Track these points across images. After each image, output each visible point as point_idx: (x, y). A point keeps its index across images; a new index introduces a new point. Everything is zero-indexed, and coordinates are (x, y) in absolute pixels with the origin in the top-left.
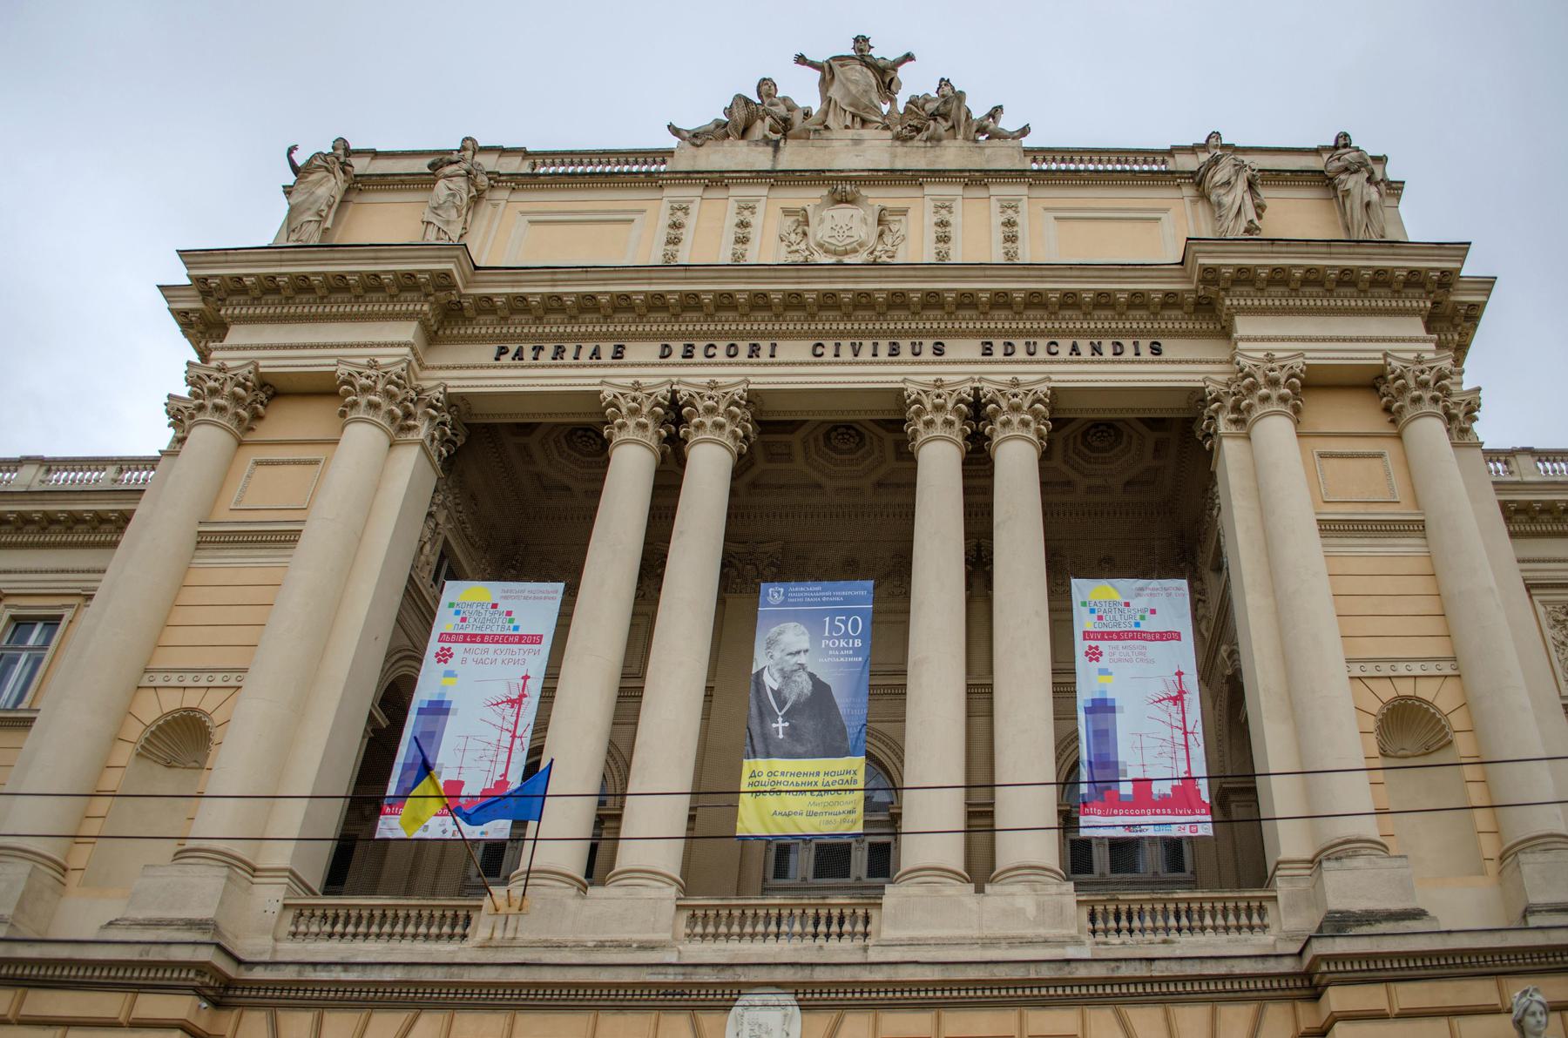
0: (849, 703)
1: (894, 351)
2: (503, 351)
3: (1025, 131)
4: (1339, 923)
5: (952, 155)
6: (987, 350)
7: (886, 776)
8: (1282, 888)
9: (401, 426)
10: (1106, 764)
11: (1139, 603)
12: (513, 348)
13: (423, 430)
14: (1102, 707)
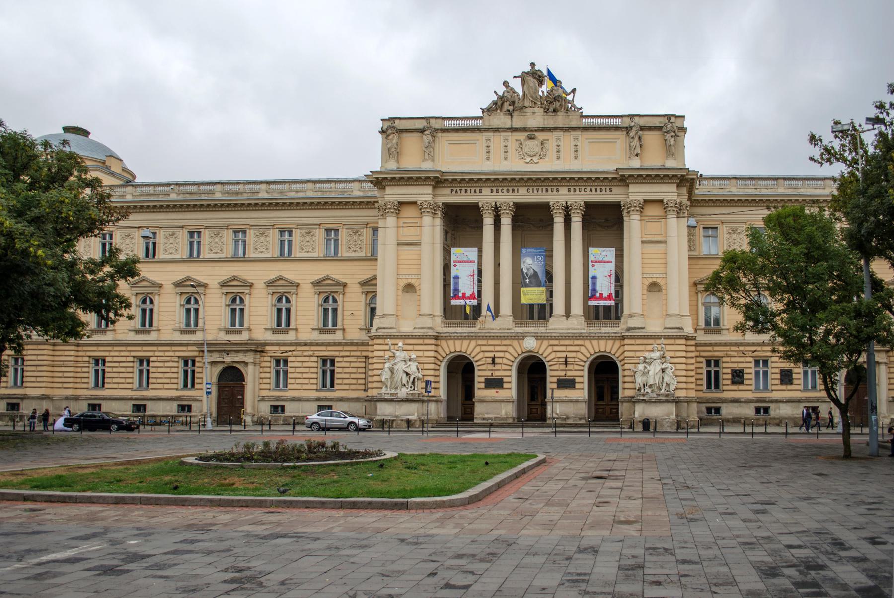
0: (542, 277)
1: (547, 191)
3: (581, 108)
4: (629, 329)
6: (569, 190)
7: (551, 294)
8: (622, 320)
10: (594, 290)
11: (604, 254)
14: (594, 278)
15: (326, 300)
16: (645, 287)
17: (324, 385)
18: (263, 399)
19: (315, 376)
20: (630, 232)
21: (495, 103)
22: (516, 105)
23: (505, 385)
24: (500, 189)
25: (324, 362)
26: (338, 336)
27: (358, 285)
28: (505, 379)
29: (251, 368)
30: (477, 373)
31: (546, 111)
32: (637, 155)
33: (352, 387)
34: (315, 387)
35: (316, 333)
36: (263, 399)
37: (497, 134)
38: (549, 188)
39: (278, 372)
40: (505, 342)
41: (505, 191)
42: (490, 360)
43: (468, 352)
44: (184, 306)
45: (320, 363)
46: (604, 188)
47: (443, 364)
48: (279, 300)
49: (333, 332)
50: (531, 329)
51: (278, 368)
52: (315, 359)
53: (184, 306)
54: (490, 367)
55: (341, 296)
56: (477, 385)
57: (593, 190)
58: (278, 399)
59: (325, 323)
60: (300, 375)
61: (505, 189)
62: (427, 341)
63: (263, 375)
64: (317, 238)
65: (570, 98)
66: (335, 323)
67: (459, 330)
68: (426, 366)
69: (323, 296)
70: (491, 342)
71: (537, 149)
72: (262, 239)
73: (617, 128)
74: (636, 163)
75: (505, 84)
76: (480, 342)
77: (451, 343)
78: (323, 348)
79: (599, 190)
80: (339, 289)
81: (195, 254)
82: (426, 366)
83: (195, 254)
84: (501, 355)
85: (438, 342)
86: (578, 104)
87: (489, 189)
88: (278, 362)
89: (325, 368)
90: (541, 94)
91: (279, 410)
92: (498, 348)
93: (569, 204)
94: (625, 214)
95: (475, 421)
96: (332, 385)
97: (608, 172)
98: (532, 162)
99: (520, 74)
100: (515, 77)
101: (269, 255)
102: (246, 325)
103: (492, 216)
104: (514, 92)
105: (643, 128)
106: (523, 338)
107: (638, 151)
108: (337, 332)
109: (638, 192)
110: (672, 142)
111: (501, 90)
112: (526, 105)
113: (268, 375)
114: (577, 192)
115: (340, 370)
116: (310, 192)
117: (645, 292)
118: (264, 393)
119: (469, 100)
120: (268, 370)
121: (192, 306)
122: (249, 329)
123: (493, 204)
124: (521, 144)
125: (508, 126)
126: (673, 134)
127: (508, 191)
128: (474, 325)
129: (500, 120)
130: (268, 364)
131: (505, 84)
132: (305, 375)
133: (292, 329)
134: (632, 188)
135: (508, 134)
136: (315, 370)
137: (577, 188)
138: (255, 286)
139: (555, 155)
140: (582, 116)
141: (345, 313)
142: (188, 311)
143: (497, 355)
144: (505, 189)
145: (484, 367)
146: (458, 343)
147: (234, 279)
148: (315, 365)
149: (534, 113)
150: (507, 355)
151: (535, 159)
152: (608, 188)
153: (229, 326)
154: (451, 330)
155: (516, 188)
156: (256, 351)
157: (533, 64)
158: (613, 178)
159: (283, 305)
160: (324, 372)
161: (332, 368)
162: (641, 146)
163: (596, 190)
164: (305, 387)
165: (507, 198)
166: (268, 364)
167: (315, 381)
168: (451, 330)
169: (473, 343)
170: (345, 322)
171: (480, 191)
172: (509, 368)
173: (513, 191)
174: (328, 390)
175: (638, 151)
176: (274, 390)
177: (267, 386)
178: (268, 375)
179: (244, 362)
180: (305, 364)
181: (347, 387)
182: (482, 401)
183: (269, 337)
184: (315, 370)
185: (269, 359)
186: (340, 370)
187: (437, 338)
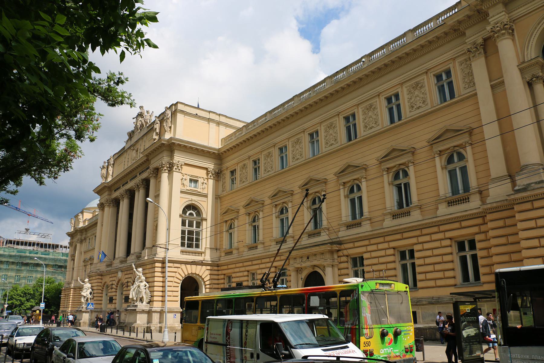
25: (461, 246)
34: (451, 282)
39: (404, 267)
52: (448, 242)
60: (430, 268)
64: (427, 88)
89: (463, 254)
108: (472, 198)
160: (463, 260)
161: (473, 252)
164: (439, 283)
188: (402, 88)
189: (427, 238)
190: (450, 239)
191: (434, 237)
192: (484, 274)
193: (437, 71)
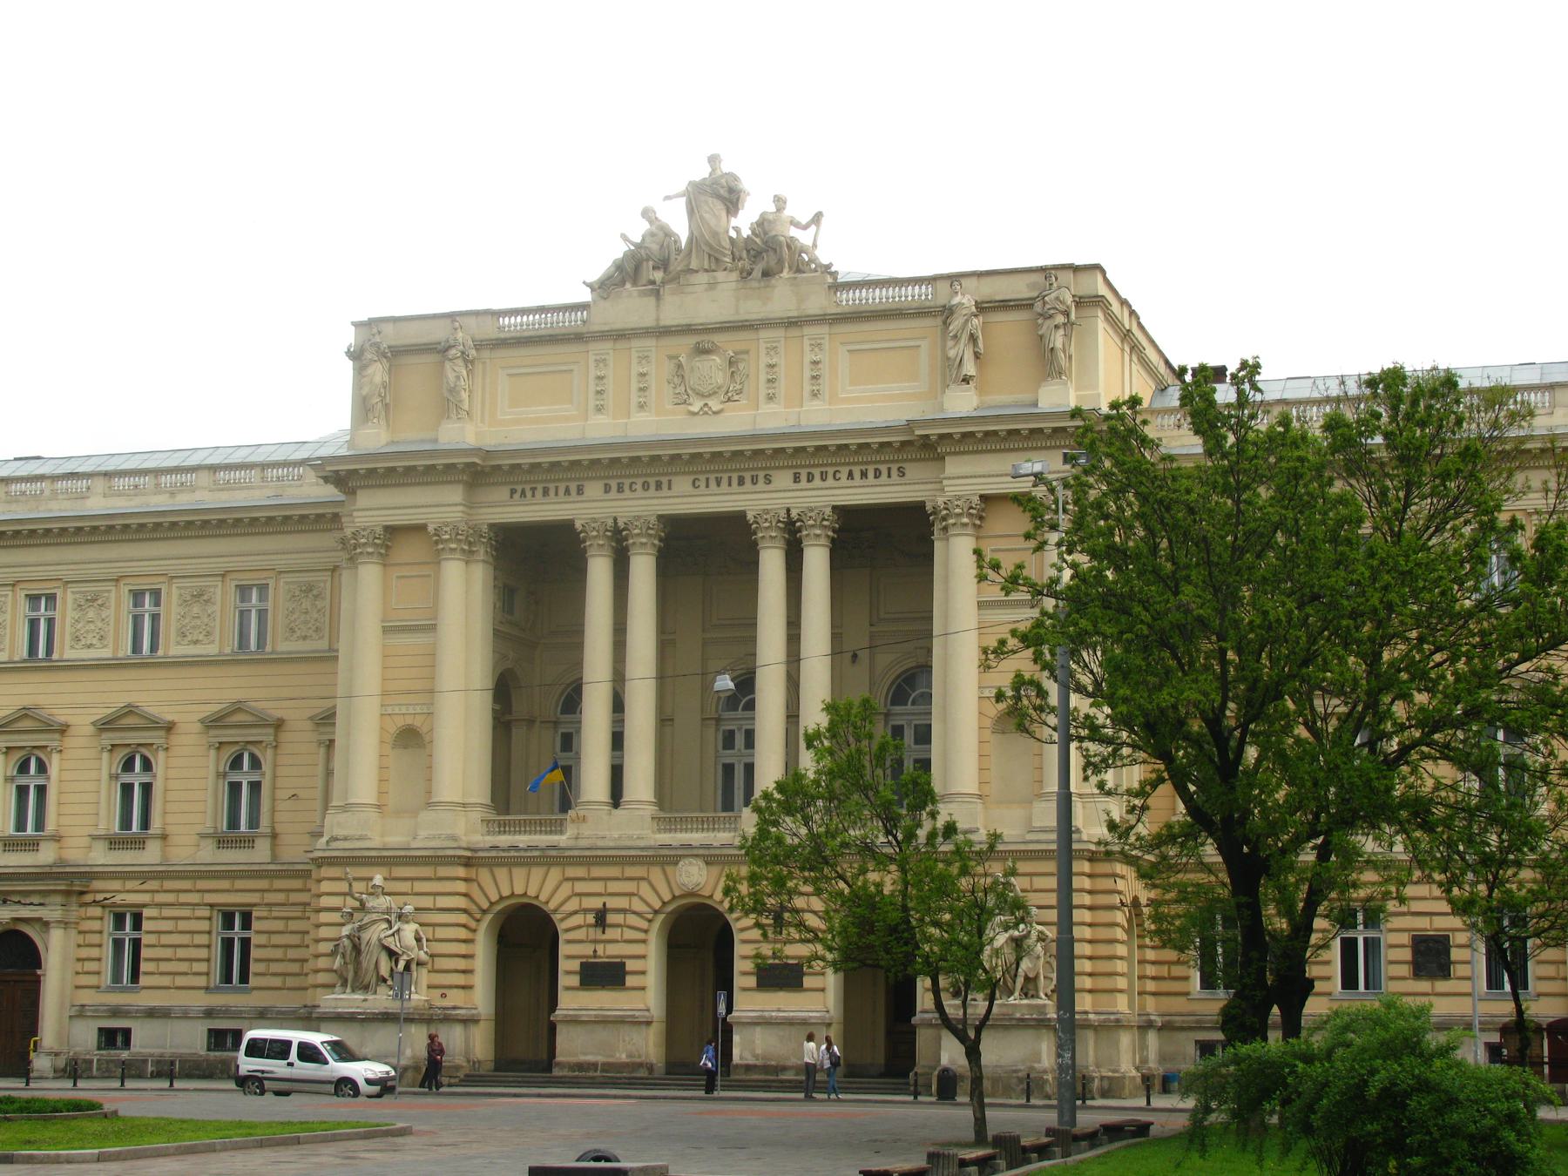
2: (513, 492)
5: (781, 299)
6: (797, 479)
9: (468, 556)
12: (519, 488)
13: (481, 555)
15: (236, 763)
16: (988, 723)
17: (227, 978)
18: (81, 1013)
19: (203, 953)
20: (946, 579)
21: (619, 266)
22: (671, 268)
23: (630, 981)
24: (627, 482)
26: (260, 853)
27: (309, 725)
28: (631, 965)
29: (56, 937)
30: (564, 949)
31: (746, 275)
32: (966, 380)
33: (290, 982)
34: (202, 981)
35: (209, 845)
36: (81, 1013)
37: (621, 345)
38: (747, 476)
39: (118, 944)
40: (631, 871)
41: (639, 487)
42: (591, 919)
43: (543, 898)
44: (117, 777)
45: (218, 921)
46: (883, 468)
47: (484, 925)
48: (128, 766)
49: (248, 842)
50: (696, 837)
51: (119, 935)
52: (206, 912)
53: (117, 777)
54: (595, 933)
55: (269, 752)
56: (563, 980)
57: (857, 475)
58: (116, 1012)
59: (234, 822)
60: (168, 953)
61: (640, 481)
62: (443, 871)
63: (85, 953)
64: (217, 607)
65: (804, 238)
66: (254, 822)
67: (523, 840)
68: (442, 933)
69: (228, 752)
70: (597, 871)
71: (720, 378)
72: (91, 614)
73: (921, 312)
74: (962, 403)
75: (647, 214)
76: (572, 872)
77: (501, 873)
78: (225, 884)
79: (871, 474)
80: (266, 735)
81: (41, 653)
82: (442, 933)
83: (41, 653)
84: (622, 903)
85: (472, 873)
86: (823, 257)
87: (600, 485)
88: (119, 920)
89: (229, 933)
90: (733, 234)
91: (119, 1039)
92: (614, 887)
93: (794, 514)
94: (937, 533)
95: (556, 1072)
96: (244, 978)
97: (888, 429)
98: (705, 411)
99: (682, 187)
100: (667, 198)
101: (106, 653)
102: (51, 826)
103: (607, 551)
104: (668, 233)
105: (982, 308)
106: (674, 861)
107: (970, 368)
109: (965, 478)
110: (1058, 340)
111: (638, 230)
112: (694, 265)
113: (95, 952)
114: (817, 482)
115: (262, 939)
116: (204, 497)
117: (987, 734)
118: (87, 997)
119: (553, 263)
120: (95, 939)
121: (32, 781)
122: (57, 838)
123: (610, 522)
124: (680, 366)
125: (648, 321)
126: (1060, 319)
127: (646, 486)
128: (559, 827)
129: (633, 309)
130: (96, 925)
131: (647, 214)
132: (181, 953)
133: (155, 837)
134: (953, 466)
135: (650, 343)
136: (204, 939)
137: (816, 472)
138: (72, 731)
139: (763, 391)
140: (838, 287)
141: (281, 794)
142: (22, 791)
143: (612, 903)
144: (640, 481)
145: (580, 934)
146: (519, 873)
147: (25, 713)
148: (205, 925)
149: (712, 286)
150: (637, 905)
151: (715, 404)
152: (894, 468)
153: (116, 828)
154: (504, 840)
155: (665, 480)
156: (67, 893)
157: (713, 160)
158: (904, 444)
159: (137, 778)
160: (228, 944)
161: (246, 934)
162: (977, 356)
163: (864, 475)
164: (180, 981)
165: (642, 506)
166: (96, 925)
167: (202, 967)
168: (504, 840)
169: (555, 874)
170: (279, 817)
171: (580, 491)
172: (641, 936)
173: (659, 486)
174: (236, 990)
175: (970, 368)
176: (110, 990)
177: (92, 980)
178: (95, 952)
179: (39, 920)
180: (182, 925)
181: (277, 982)
182: (574, 1021)
183: (101, 857)
184: (204, 939)
185: (97, 911)
186: (262, 939)
187: (468, 863)
188: (170, 586)
189: (170, 898)
190: (212, 906)
191: (184, 898)
192: (256, 974)
193: (247, 579)
